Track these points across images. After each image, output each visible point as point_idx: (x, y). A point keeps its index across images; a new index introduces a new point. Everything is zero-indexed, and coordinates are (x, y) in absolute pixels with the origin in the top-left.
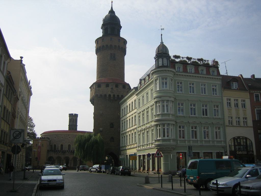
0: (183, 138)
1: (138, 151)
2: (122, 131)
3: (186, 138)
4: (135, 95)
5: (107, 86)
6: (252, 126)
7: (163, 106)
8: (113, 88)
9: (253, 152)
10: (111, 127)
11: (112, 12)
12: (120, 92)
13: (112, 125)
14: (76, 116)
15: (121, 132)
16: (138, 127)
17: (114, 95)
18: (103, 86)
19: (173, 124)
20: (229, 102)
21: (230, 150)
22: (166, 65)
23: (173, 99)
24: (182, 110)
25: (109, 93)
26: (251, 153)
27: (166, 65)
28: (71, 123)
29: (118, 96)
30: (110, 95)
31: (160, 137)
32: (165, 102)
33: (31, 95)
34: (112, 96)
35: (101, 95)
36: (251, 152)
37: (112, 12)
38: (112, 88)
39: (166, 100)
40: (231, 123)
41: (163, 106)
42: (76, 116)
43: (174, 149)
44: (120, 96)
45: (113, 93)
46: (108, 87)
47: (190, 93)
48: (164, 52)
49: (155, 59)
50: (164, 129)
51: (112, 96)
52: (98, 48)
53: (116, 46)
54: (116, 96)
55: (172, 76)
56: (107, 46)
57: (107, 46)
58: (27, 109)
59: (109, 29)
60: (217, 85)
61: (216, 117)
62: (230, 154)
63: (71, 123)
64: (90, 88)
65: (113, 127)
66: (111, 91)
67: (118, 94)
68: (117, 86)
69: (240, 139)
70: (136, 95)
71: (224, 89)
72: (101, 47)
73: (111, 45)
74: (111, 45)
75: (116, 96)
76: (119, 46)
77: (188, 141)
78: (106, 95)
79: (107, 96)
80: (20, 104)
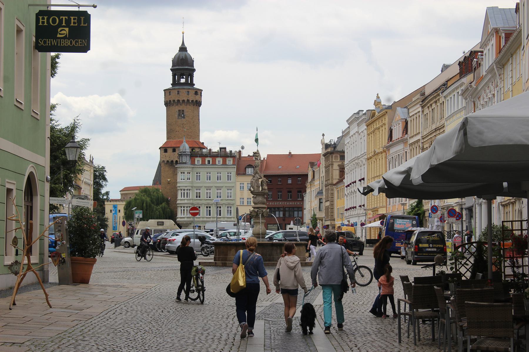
5: (174, 150)
11: (183, 49)
18: (170, 151)
32: (183, 190)
35: (168, 161)
37: (183, 49)
43: (191, 224)
46: (175, 152)
53: (183, 101)
55: (191, 170)
57: (174, 101)
61: (229, 198)
72: (168, 102)
73: (178, 101)
76: (188, 100)
78: (172, 161)
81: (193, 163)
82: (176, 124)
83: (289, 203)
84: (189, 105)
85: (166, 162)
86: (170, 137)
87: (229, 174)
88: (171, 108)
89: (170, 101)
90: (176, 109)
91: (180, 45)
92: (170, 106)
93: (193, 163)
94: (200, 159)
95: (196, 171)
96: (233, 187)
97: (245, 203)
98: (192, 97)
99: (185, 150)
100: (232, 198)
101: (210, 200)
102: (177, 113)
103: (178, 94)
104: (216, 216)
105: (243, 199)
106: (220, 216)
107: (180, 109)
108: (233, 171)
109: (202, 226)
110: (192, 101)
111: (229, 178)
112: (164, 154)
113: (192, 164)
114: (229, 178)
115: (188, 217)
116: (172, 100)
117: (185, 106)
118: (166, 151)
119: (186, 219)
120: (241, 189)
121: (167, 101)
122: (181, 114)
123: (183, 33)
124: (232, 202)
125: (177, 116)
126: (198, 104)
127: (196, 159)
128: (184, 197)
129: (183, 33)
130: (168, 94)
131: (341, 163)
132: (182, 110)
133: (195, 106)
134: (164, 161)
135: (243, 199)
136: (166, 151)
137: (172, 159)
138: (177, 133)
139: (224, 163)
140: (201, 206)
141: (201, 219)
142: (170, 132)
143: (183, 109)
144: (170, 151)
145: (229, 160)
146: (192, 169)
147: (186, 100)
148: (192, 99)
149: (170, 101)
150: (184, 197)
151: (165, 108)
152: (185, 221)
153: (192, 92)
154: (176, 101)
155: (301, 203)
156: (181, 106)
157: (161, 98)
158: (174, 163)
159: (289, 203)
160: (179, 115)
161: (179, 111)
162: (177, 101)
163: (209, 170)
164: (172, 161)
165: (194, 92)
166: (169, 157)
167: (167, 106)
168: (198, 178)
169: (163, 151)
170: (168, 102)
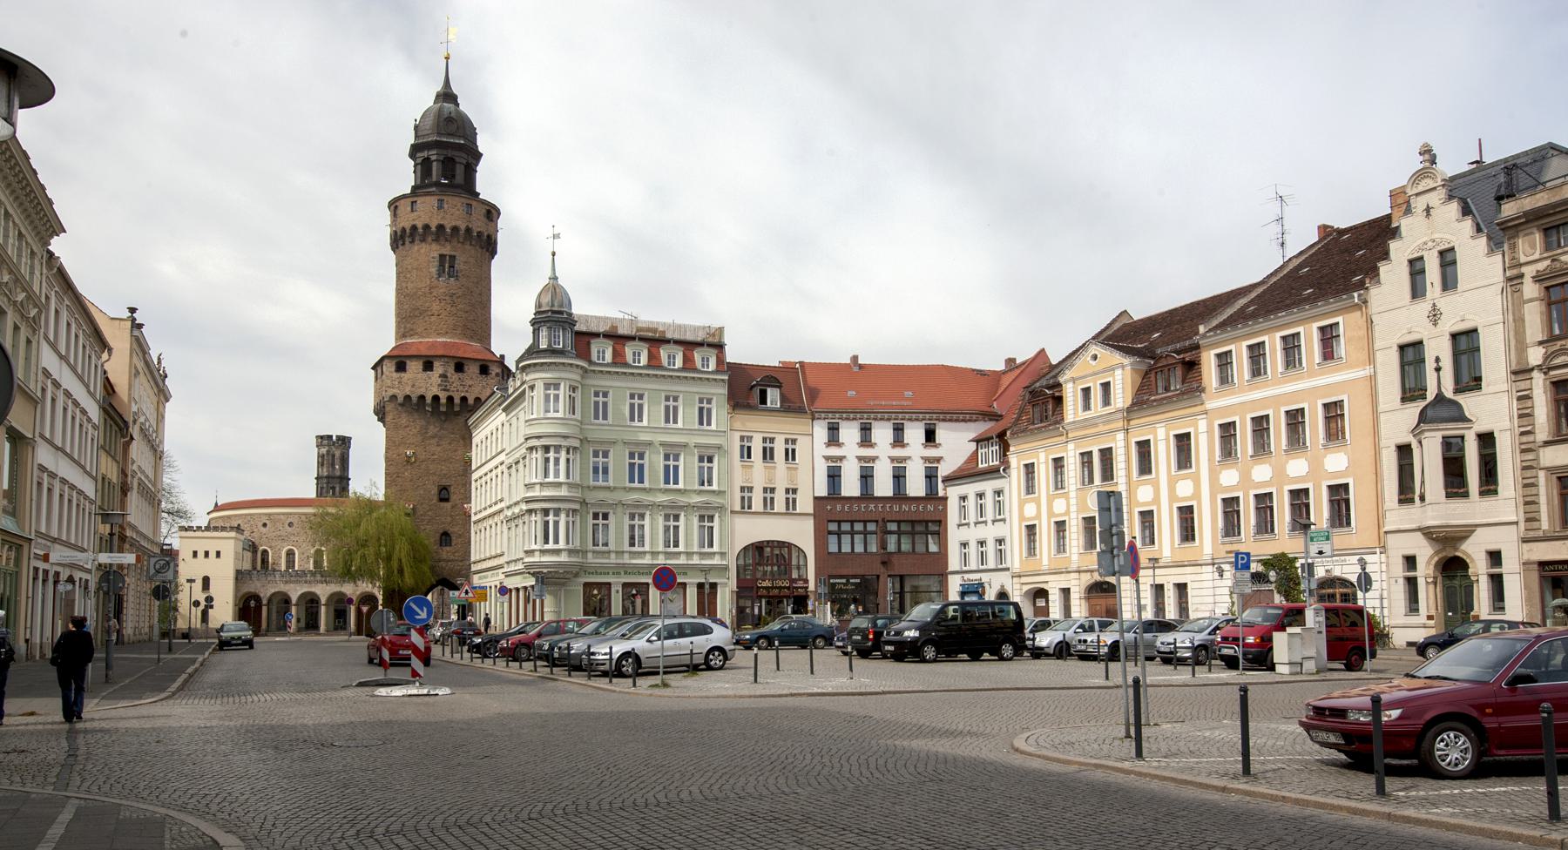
0: (606, 544)
1: (506, 576)
2: (476, 514)
3: (612, 547)
4: (500, 411)
5: (428, 366)
6: (812, 512)
7: (547, 460)
8: (449, 375)
9: (806, 581)
10: (442, 500)
12: (470, 386)
13: (444, 494)
14: (345, 442)
15: (473, 515)
16: (508, 508)
17: (450, 399)
18: (414, 367)
19: (574, 511)
20: (747, 444)
21: (742, 576)
22: (561, 346)
23: (579, 442)
24: (605, 471)
25: (435, 391)
26: (800, 584)
27: (561, 346)
28: (325, 470)
29: (464, 399)
30: (436, 398)
31: (536, 544)
32: (552, 450)
33: (167, 400)
34: (443, 401)
35: (408, 398)
36: (801, 582)
38: (443, 376)
39: (555, 446)
40: (746, 504)
41: (547, 460)
42: (345, 442)
43: (577, 575)
44: (471, 401)
45: (448, 390)
46: (432, 370)
47: (629, 423)
48: (556, 309)
49: (532, 325)
50: (546, 523)
51: (443, 401)
52: (399, 233)
54: (457, 401)
56: (427, 227)
57: (427, 227)
58: (156, 451)
59: (435, 163)
60: (715, 399)
61: (706, 487)
62: (737, 588)
63: (325, 470)
64: (373, 368)
65: (447, 500)
66: (439, 385)
67: (463, 395)
68: (459, 367)
69: (772, 548)
70: (504, 410)
71: (733, 410)
72: (408, 231)
73: (441, 227)
74: (441, 227)
75: (457, 401)
76: (468, 230)
77: (617, 552)
78: (422, 398)
79: (429, 400)
80: (138, 451)
82: (431, 293)
83: (900, 508)
84: (471, 245)
85: (401, 399)
86: (412, 330)
87: (705, 405)
88: (416, 248)
89: (414, 228)
90: (428, 253)
91: (439, 87)
92: (412, 242)
93: (584, 353)
95: (594, 386)
96: (719, 447)
98: (478, 224)
99: (561, 306)
100: (715, 487)
101: (645, 489)
102: (437, 264)
103: (440, 207)
104: (661, 548)
105: (750, 489)
106: (676, 550)
107: (445, 253)
109: (617, 583)
110: (480, 234)
111: (704, 416)
112: (395, 375)
113: (578, 356)
114: (704, 416)
115: (543, 552)
116: (420, 226)
117: (460, 245)
118: (401, 367)
119: (563, 558)
120: (742, 456)
121: (404, 230)
122: (447, 265)
123: (447, 58)
125: (434, 270)
126: (488, 246)
128: (557, 474)
129: (447, 58)
130: (409, 209)
131: (1548, 262)
132: (450, 256)
133: (484, 250)
134: (394, 397)
135: (750, 489)
136: (401, 367)
137: (421, 391)
138: (433, 318)
139: (688, 364)
140: (611, 511)
141: (613, 559)
142: (409, 314)
143: (453, 253)
144: (414, 367)
145: (558, 411)
146: (582, 377)
147: (463, 227)
148: (479, 230)
149: (414, 228)
150: (557, 474)
151: (392, 257)
152: (560, 565)
153: (479, 212)
154: (434, 229)
155: (940, 508)
156: (447, 244)
157: (381, 227)
158: (429, 400)
159: (900, 508)
160: (442, 264)
161: (442, 257)
162: (437, 227)
163: (639, 385)
164: (422, 398)
165: (484, 211)
166: (413, 386)
167: (403, 244)
168: (601, 411)
169: (393, 369)
170: (408, 231)
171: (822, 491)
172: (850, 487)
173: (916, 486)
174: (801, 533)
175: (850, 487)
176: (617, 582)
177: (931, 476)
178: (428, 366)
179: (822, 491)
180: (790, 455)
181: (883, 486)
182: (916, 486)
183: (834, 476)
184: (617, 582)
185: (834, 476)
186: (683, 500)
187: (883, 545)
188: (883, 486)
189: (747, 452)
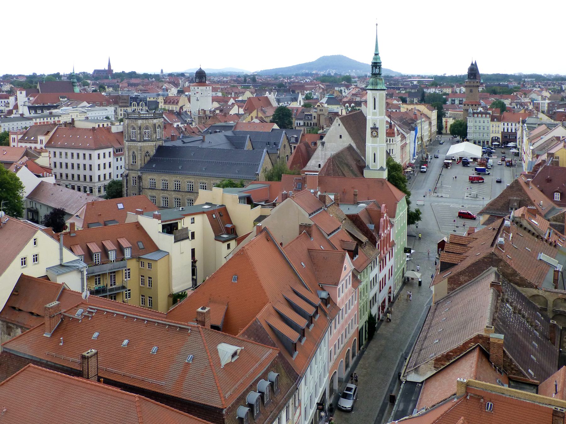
5: (468, 105)
18: (466, 105)
40: (493, 132)
81: (474, 116)
93: (474, 116)
94: (476, 115)
97: (494, 132)
108: (490, 119)
124: (489, 132)
127: (475, 115)
144: (466, 105)
163: (479, 119)
168: (476, 122)
171: (502, 131)
172: (506, 131)
173: (514, 131)
174: (500, 136)
175: (506, 131)
176: (477, 140)
177: (516, 129)
178: (468, 105)
179: (502, 131)
180: (499, 127)
181: (510, 131)
182: (514, 131)
183: (504, 129)
184: (477, 140)
185: (504, 129)
186: (485, 132)
187: (509, 137)
188: (510, 131)
189: (493, 126)
